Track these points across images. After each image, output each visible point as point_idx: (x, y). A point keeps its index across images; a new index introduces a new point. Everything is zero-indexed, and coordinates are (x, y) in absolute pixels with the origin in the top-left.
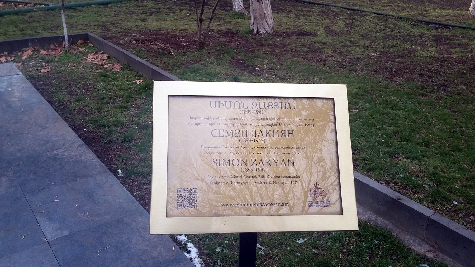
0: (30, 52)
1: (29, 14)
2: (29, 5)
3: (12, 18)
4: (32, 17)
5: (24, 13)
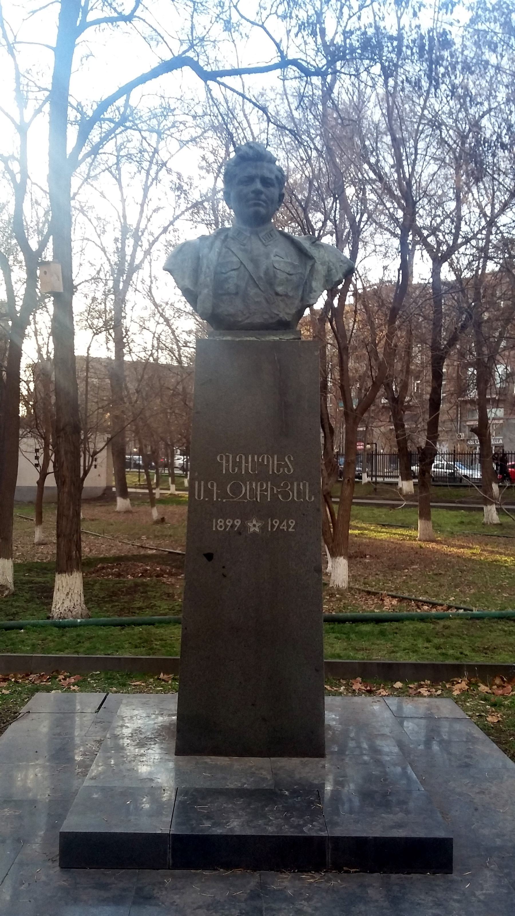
0: (464, 685)
1: (442, 623)
2: (439, 608)
3: (417, 626)
4: (446, 627)
5: (434, 620)
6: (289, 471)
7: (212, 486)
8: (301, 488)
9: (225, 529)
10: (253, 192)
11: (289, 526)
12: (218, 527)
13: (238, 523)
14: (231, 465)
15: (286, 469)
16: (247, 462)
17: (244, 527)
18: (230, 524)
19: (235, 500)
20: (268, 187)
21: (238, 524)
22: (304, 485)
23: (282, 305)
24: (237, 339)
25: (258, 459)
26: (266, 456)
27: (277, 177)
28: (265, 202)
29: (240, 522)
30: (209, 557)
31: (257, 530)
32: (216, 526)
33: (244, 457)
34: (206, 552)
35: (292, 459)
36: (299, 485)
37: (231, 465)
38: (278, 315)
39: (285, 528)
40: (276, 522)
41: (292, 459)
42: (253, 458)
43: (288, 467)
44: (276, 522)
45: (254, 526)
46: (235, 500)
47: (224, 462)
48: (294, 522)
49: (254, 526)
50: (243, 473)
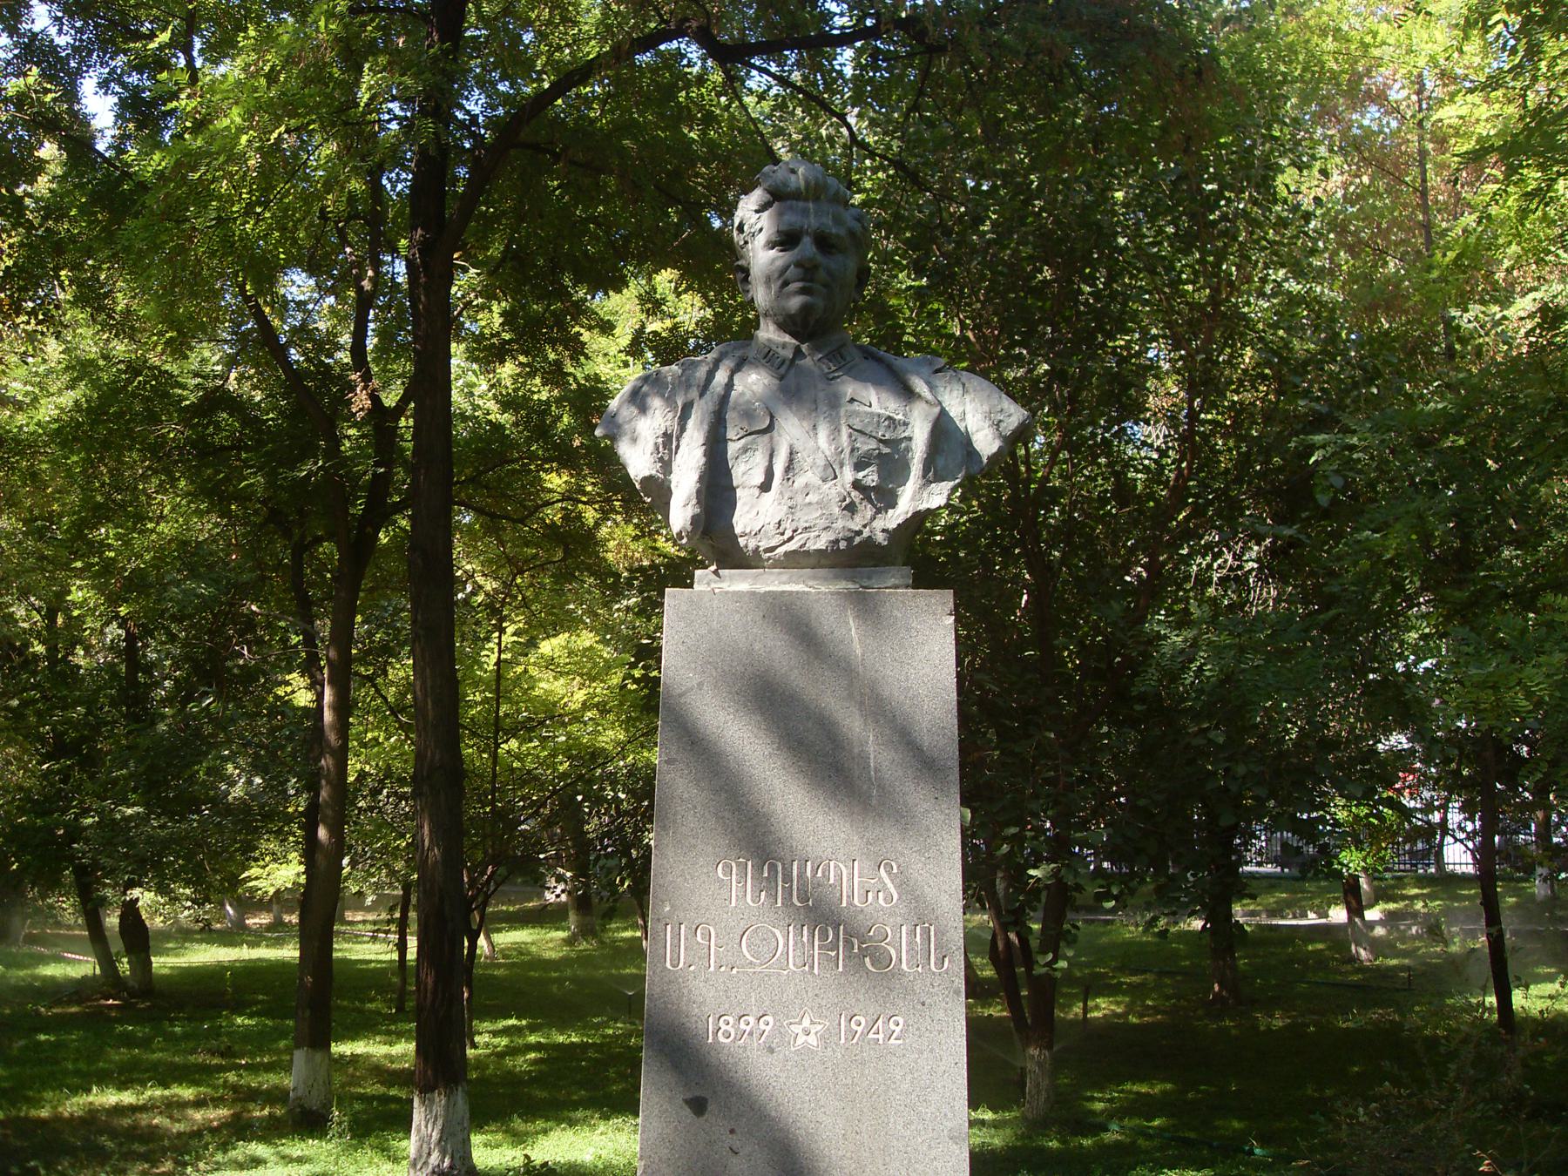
17: (779, 1031)
18: (748, 1029)
19: (758, 969)
20: (830, 253)
21: (768, 1028)
26: (832, 863)
27: (852, 233)
28: (825, 286)
29: (771, 1024)
31: (812, 1040)
35: (895, 871)
39: (881, 1036)
41: (895, 871)
43: (885, 888)
48: (901, 1021)
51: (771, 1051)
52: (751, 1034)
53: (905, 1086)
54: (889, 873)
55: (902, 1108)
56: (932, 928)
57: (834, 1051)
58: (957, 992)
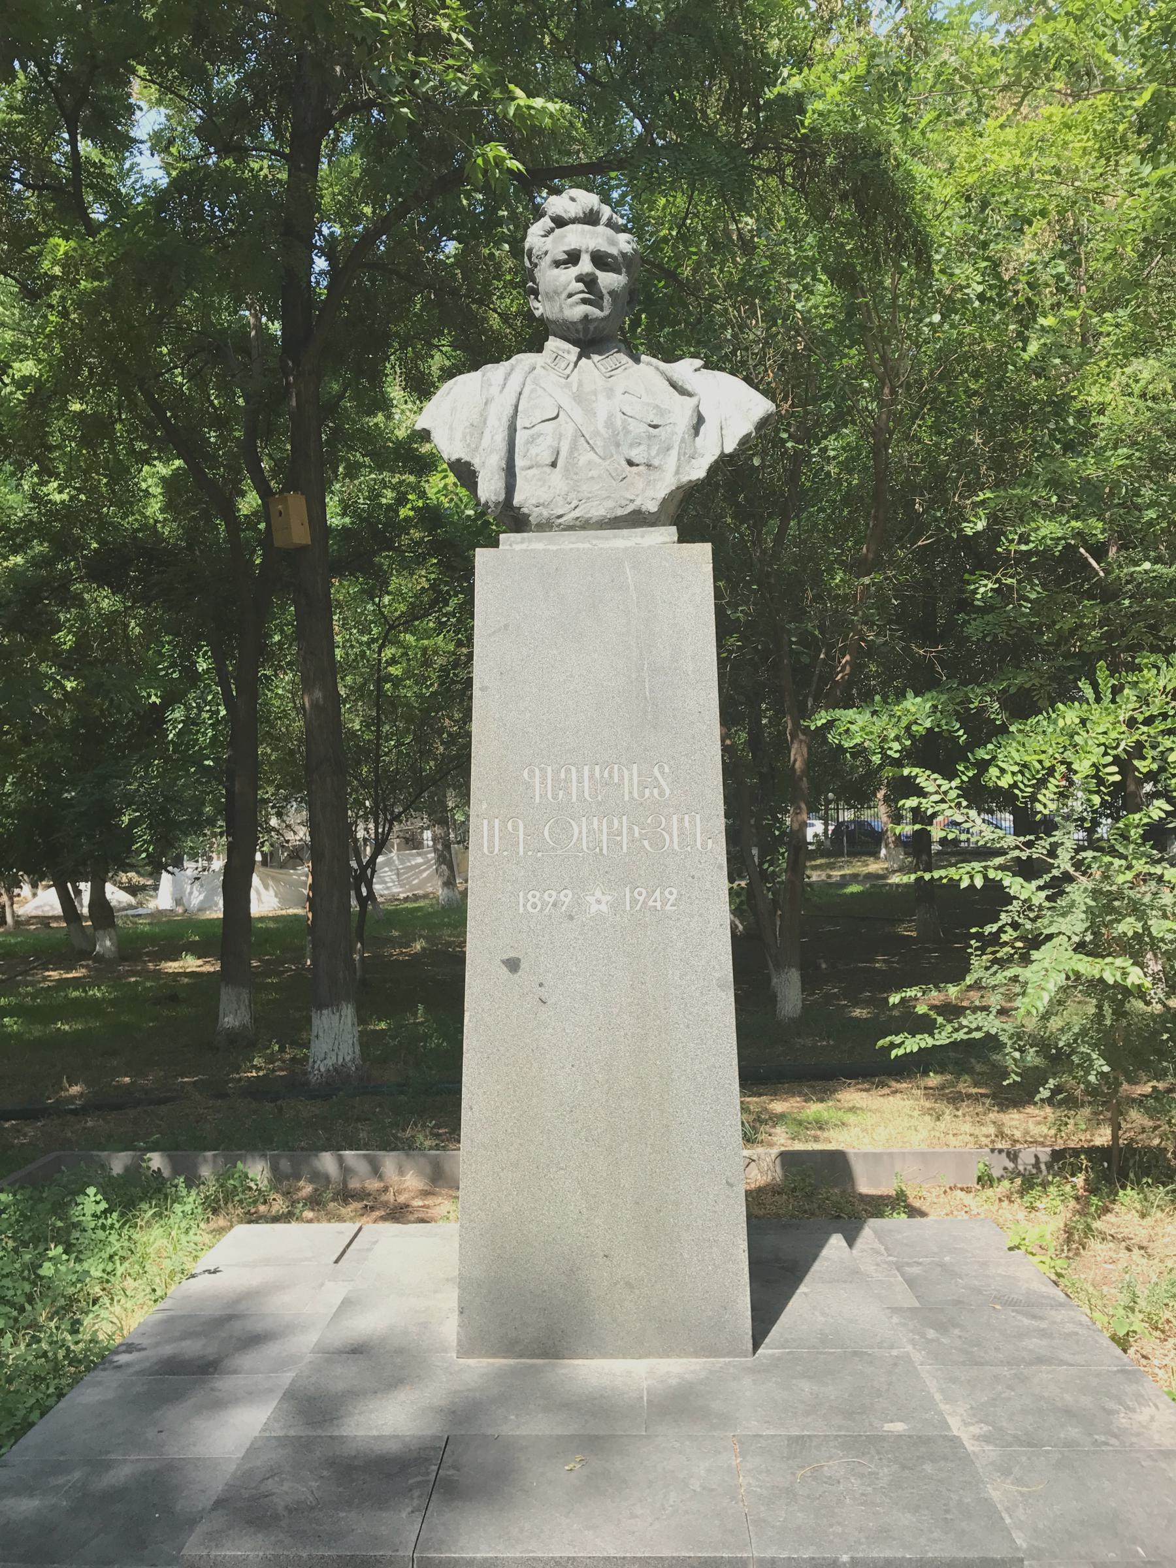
6: (662, 794)
7: (515, 828)
8: (687, 824)
9: (542, 910)
10: (579, 279)
11: (665, 902)
12: (529, 905)
13: (567, 897)
14: (549, 786)
15: (656, 791)
16: (580, 781)
18: (552, 901)
19: (559, 852)
21: (567, 900)
22: (692, 821)
23: (640, 484)
24: (553, 548)
25: (601, 772)
29: (570, 896)
30: (513, 965)
31: (604, 908)
32: (524, 905)
33: (574, 769)
34: (506, 957)
35: (667, 770)
36: (681, 820)
37: (549, 786)
38: (632, 501)
39: (658, 904)
40: (640, 894)
41: (667, 770)
42: (592, 771)
43: (659, 786)
44: (640, 894)
45: (599, 902)
46: (559, 852)
47: (537, 780)
48: (675, 891)
49: (599, 902)
50: (574, 800)
51: (571, 918)
52: (554, 905)
53: (680, 944)
54: (662, 773)
55: (678, 962)
56: (698, 816)
57: (622, 917)
58: (720, 867)
